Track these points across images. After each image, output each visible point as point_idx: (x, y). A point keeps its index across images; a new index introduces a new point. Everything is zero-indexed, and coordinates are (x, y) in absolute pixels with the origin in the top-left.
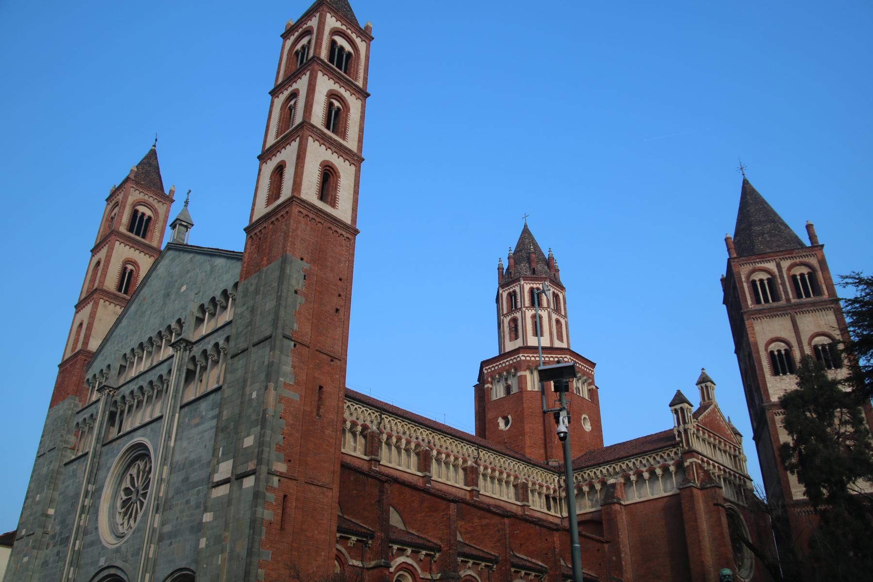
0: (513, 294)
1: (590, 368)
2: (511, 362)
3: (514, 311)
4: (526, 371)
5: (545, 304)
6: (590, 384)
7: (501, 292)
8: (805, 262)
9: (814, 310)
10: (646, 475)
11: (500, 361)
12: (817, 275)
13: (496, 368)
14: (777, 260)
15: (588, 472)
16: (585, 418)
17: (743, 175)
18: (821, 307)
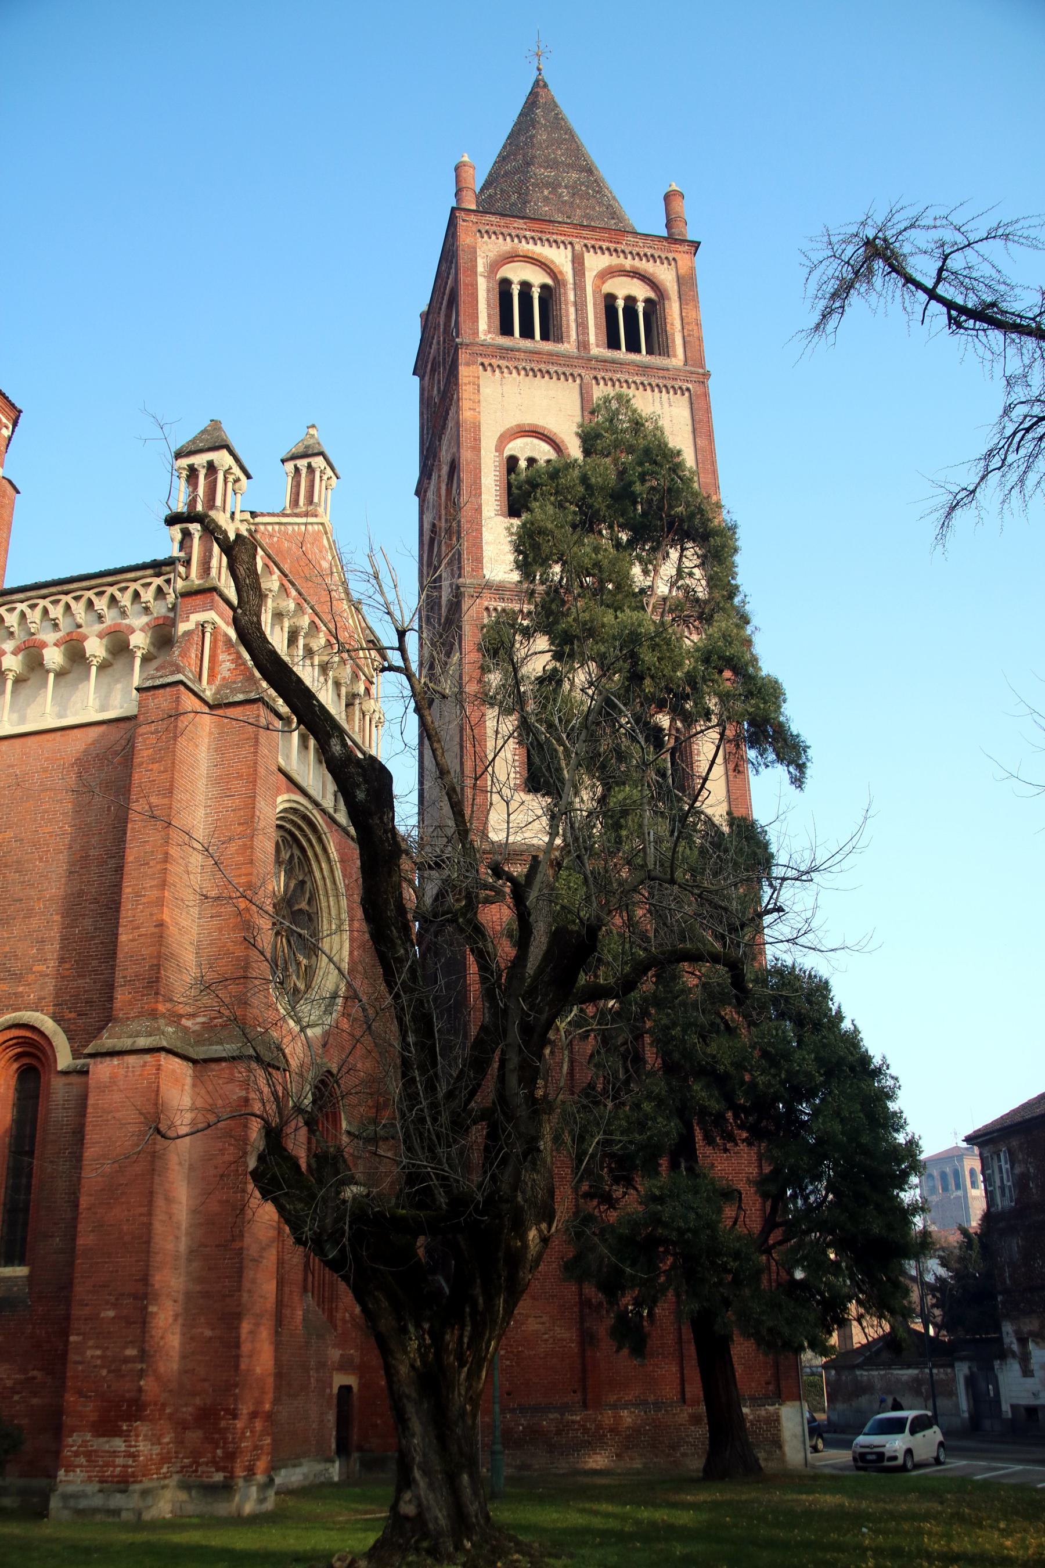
8: (646, 271)
9: (642, 383)
10: (53, 657)
12: (667, 306)
14: (577, 247)
17: (539, 69)
18: (661, 383)
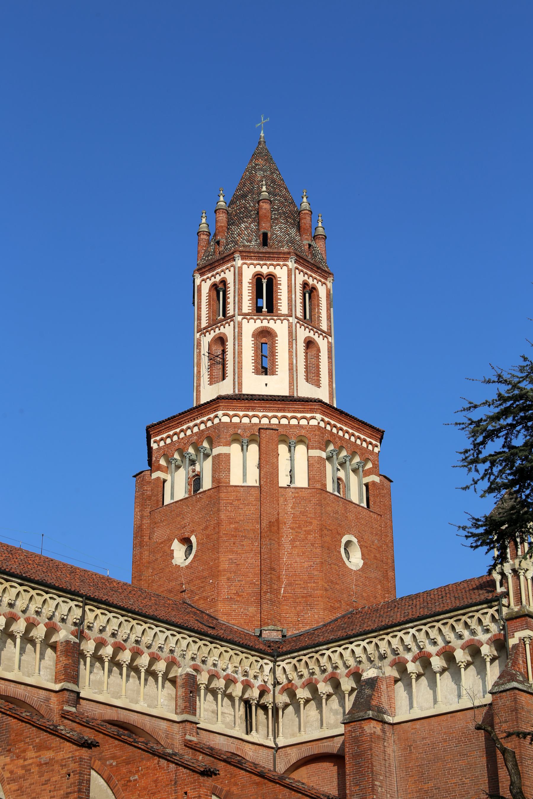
0: (221, 286)
1: (368, 440)
2: (202, 427)
3: (222, 321)
4: (229, 444)
5: (283, 307)
6: (367, 473)
7: (198, 281)
11: (182, 425)
13: (175, 438)
15: (328, 653)
16: (348, 543)
